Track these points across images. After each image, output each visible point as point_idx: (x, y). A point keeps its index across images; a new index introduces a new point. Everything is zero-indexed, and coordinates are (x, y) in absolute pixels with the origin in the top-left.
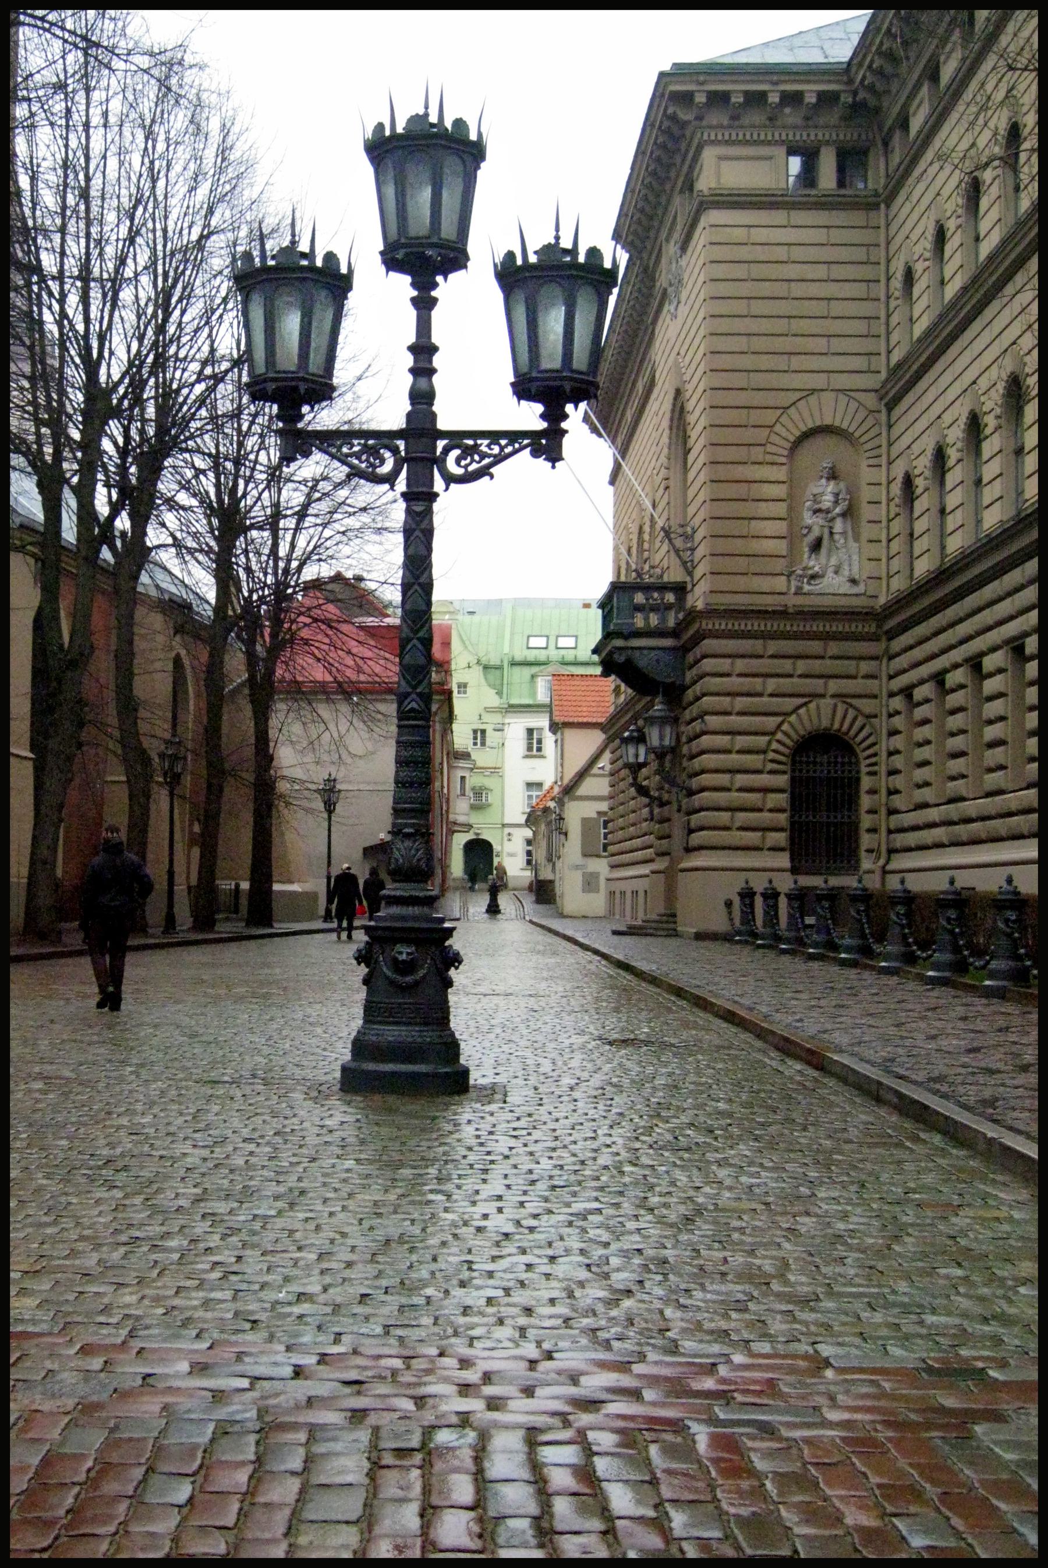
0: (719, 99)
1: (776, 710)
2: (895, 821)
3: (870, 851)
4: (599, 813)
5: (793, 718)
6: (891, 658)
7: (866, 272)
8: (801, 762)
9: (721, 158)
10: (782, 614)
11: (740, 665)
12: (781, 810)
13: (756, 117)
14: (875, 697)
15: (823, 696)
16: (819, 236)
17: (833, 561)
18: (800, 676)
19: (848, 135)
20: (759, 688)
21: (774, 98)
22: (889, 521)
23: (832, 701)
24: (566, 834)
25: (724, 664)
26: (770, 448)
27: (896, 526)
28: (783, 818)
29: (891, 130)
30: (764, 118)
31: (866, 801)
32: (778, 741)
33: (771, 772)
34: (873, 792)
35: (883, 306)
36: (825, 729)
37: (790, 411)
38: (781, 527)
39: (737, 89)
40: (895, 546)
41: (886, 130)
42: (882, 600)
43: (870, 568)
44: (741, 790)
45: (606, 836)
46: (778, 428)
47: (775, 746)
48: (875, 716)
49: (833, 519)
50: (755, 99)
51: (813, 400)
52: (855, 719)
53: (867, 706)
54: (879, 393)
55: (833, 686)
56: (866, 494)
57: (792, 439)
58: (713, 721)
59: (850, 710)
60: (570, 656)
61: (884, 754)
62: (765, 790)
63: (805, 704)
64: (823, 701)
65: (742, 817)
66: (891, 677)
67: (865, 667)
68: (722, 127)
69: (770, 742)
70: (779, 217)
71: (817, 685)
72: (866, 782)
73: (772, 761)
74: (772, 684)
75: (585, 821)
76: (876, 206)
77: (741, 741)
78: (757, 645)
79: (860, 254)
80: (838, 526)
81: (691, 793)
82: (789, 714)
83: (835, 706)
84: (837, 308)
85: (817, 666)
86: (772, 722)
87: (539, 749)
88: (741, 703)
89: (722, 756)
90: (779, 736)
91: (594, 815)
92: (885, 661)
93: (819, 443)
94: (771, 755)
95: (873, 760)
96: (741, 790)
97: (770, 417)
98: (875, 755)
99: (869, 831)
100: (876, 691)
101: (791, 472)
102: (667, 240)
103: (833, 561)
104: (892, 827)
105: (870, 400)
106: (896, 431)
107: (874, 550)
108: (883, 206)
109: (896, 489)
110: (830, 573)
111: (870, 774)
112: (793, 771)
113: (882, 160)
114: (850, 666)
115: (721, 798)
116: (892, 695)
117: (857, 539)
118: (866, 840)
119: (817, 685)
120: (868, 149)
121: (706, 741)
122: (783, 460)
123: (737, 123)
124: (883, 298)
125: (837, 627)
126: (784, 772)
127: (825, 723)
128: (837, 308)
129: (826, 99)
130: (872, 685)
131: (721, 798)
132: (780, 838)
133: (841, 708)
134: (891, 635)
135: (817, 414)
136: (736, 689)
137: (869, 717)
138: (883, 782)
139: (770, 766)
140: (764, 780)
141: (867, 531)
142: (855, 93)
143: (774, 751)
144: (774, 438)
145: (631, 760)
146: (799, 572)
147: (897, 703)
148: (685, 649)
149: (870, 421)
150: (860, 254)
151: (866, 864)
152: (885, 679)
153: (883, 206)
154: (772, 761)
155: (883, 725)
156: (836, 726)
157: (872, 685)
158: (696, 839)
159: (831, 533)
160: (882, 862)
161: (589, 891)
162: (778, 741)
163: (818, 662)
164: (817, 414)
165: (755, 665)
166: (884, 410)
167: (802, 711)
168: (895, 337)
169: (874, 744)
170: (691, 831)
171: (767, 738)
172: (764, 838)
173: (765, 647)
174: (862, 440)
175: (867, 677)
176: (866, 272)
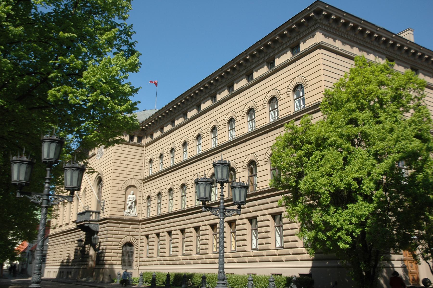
7: (141, 158)
11: (114, 229)
16: (134, 150)
27: (144, 205)
31: (135, 256)
33: (119, 249)
40: (144, 208)
54: (143, 180)
55: (131, 233)
61: (139, 247)
62: (118, 253)
67: (136, 230)
72: (135, 252)
74: (120, 233)
76: (143, 147)
77: (114, 243)
78: (117, 225)
82: (122, 239)
84: (136, 164)
88: (114, 236)
93: (131, 188)
94: (119, 246)
97: (123, 182)
101: (125, 193)
104: (141, 261)
105: (140, 181)
106: (145, 188)
109: (145, 198)
110: (131, 212)
111: (136, 250)
116: (141, 236)
118: (135, 263)
128: (136, 164)
132: (120, 262)
137: (137, 239)
138: (139, 252)
147: (144, 237)
155: (139, 241)
160: (138, 267)
166: (143, 183)
168: (145, 171)
175: (137, 232)
176: (141, 158)
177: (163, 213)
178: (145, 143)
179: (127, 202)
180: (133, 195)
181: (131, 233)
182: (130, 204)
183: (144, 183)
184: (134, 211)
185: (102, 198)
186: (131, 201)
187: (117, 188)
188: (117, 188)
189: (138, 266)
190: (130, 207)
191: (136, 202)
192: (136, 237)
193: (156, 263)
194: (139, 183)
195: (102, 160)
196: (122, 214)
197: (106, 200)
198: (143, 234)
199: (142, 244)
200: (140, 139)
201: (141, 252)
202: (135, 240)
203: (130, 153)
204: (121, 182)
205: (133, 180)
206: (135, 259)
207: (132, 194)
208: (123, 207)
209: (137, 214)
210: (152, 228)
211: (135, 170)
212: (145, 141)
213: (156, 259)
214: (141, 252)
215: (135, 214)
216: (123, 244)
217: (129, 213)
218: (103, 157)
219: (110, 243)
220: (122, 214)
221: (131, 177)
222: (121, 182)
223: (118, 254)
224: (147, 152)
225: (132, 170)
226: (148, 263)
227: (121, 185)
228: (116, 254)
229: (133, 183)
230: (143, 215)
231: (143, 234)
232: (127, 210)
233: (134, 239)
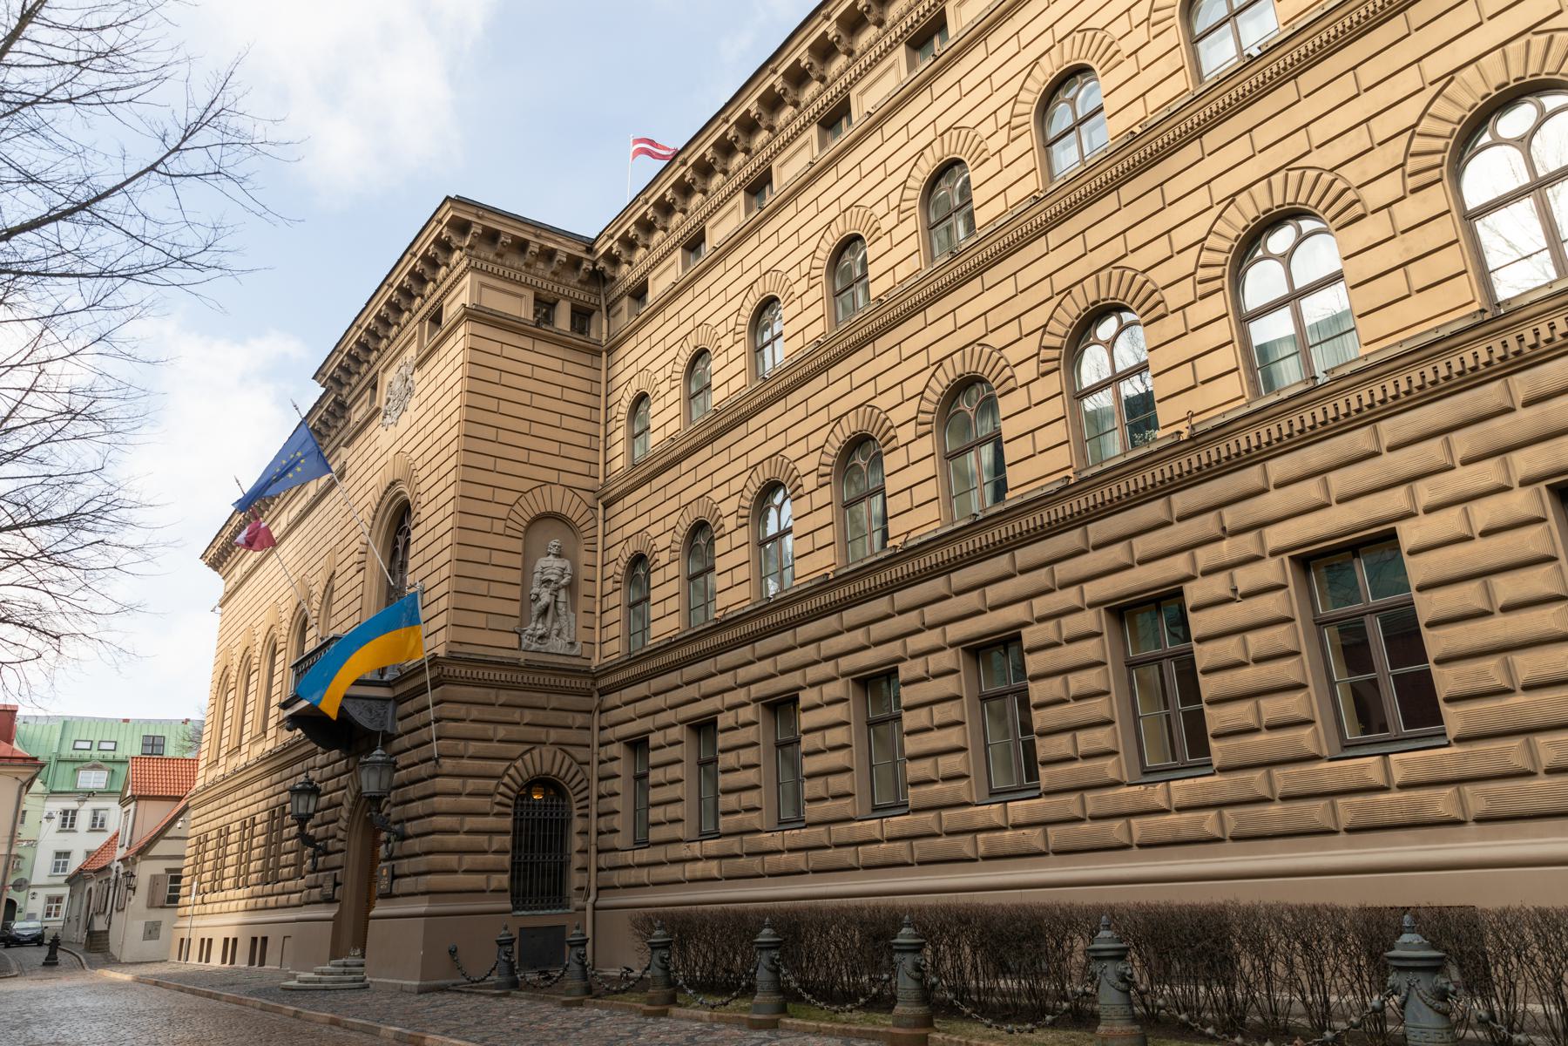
0: (491, 236)
1: (504, 755)
2: (605, 860)
3: (580, 889)
4: (168, 871)
5: (519, 763)
6: (601, 712)
7: (591, 400)
9: (483, 285)
10: (513, 665)
11: (475, 712)
12: (505, 852)
13: (516, 261)
14: (588, 746)
16: (557, 365)
17: (556, 626)
18: (527, 724)
19: (581, 295)
20: (490, 734)
21: (534, 248)
22: (603, 597)
23: (553, 748)
24: (134, 889)
25: (461, 711)
26: (509, 523)
28: (506, 860)
29: (620, 297)
30: (521, 263)
31: (577, 842)
32: (505, 785)
33: (497, 815)
34: (583, 833)
35: (602, 428)
37: (527, 495)
38: (515, 592)
39: (508, 231)
41: (611, 299)
42: (596, 661)
43: (585, 635)
44: (468, 832)
45: (171, 890)
46: (517, 507)
47: (502, 789)
48: (588, 763)
49: (557, 590)
50: (521, 246)
51: (546, 489)
52: (571, 765)
53: (581, 755)
55: (554, 735)
56: (585, 573)
57: (528, 519)
58: (447, 765)
59: (567, 757)
60: (110, 755)
61: (595, 798)
63: (530, 750)
64: (544, 749)
65: (468, 861)
66: (602, 729)
67: (580, 719)
68: (487, 260)
69: (497, 786)
70: (527, 342)
71: (541, 734)
72: (577, 824)
73: (499, 804)
74: (502, 732)
75: (154, 879)
77: (472, 784)
78: (491, 695)
79: (586, 386)
80: (562, 595)
81: (403, 837)
83: (555, 753)
84: (567, 422)
85: (540, 716)
86: (500, 766)
87: (72, 826)
88: (473, 748)
89: (452, 799)
90: (506, 780)
91: (163, 872)
92: (597, 714)
94: (499, 798)
96: (469, 832)
97: (511, 498)
98: (587, 798)
99: (579, 869)
100: (588, 741)
102: (384, 371)
103: (556, 626)
106: (616, 523)
107: (585, 620)
108: (604, 354)
111: (579, 816)
112: (515, 814)
113: (605, 322)
114: (569, 719)
115: (451, 841)
116: (601, 745)
117: (574, 610)
118: (576, 880)
119: (541, 734)
120: (593, 311)
121: (440, 783)
122: (520, 535)
123: (499, 261)
124: (602, 421)
125: (564, 682)
126: (507, 814)
127: (546, 768)
128: (567, 422)
129: (574, 263)
130: (584, 737)
131: (451, 841)
132: (503, 880)
133: (559, 756)
134: (604, 692)
135: (534, 506)
136: (468, 734)
137: (581, 764)
138: (594, 824)
139: (497, 809)
140: (490, 822)
141: (583, 603)
142: (595, 264)
143: (502, 794)
144: (513, 515)
145: (301, 811)
146: (529, 631)
147: (615, 749)
148: (399, 700)
149: (589, 515)
150: (586, 386)
151: (577, 902)
153: (604, 354)
154: (499, 804)
155: (595, 771)
156: (555, 772)
157: (584, 737)
158: (405, 885)
159: (556, 601)
160: (592, 899)
161: (151, 939)
162: (505, 785)
163: (541, 713)
164: (534, 506)
165: (488, 713)
166: (601, 507)
167: (527, 757)
169: (586, 788)
170: (394, 877)
171: (494, 782)
172: (488, 879)
173: (497, 697)
174: (583, 528)
176: (591, 400)
177: (730, 610)
178: (605, 336)
179: (535, 590)
180: (558, 556)
181: (554, 735)
182: (546, 598)
183: (606, 506)
184: (565, 631)
185: (410, 579)
186: (549, 581)
187: (484, 524)
188: (484, 524)
189: (593, 891)
190: (544, 612)
191: (571, 587)
192: (581, 755)
193: (699, 869)
194: (583, 507)
195: (405, 421)
196: (512, 641)
197: (429, 583)
198: (609, 734)
199: (606, 787)
200: (581, 316)
201: (603, 823)
203: (539, 373)
204: (501, 496)
205: (558, 491)
206: (577, 861)
207: (554, 551)
208: (514, 609)
209: (579, 644)
210: (659, 702)
211: (566, 450)
212: (600, 330)
213: (696, 849)
214: (603, 823)
215: (572, 644)
216: (526, 776)
217: (542, 637)
218: (413, 403)
219: (455, 784)
220: (512, 641)
221: (552, 476)
222: (501, 496)
224: (619, 367)
225: (554, 448)
226: (643, 875)
227: (502, 512)
228: (486, 837)
229: (558, 501)
230: (615, 646)
231: (609, 734)
232: (533, 625)
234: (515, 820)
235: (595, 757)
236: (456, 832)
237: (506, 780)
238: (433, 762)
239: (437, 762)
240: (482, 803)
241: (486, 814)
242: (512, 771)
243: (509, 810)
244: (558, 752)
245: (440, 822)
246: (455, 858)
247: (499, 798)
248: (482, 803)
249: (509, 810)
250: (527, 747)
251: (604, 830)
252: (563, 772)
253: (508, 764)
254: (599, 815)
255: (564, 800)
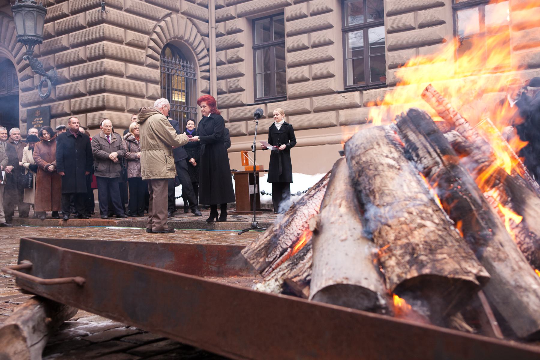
5: (163, 24)
8: (164, 62)
15: (177, 11)
32: (154, 40)
36: (181, 38)
44: (130, 77)
47: (152, 44)
48: (208, 36)
62: (148, 81)
63: (169, 15)
77: (131, 35)
81: (57, 81)
86: (150, 24)
90: (155, 36)
94: (150, 52)
95: (207, 67)
100: (207, 17)
111: (203, 78)
121: (107, 29)
127: (181, 33)
133: (190, 24)
138: (215, 85)
139: (150, 61)
147: (241, 23)
152: (213, 8)
156: (186, 38)
162: (154, 40)
167: (168, 19)
171: (147, 37)
192: (203, 26)
202: (199, 37)
219: (119, 32)
223: (151, 85)
233: (195, 30)
234: (161, 72)
235: (214, 31)
236: (121, 75)
237: (155, 36)
238: (100, 8)
239: (104, 8)
240: (140, 54)
241: (141, 64)
242: (158, 30)
243: (158, 63)
244: (188, 21)
245: (109, 63)
246: (124, 97)
247: (150, 52)
248: (140, 54)
249: (158, 63)
250: (168, 12)
251: (225, 89)
252: (192, 39)
253: (155, 22)
254: (219, 79)
255: (190, 64)
